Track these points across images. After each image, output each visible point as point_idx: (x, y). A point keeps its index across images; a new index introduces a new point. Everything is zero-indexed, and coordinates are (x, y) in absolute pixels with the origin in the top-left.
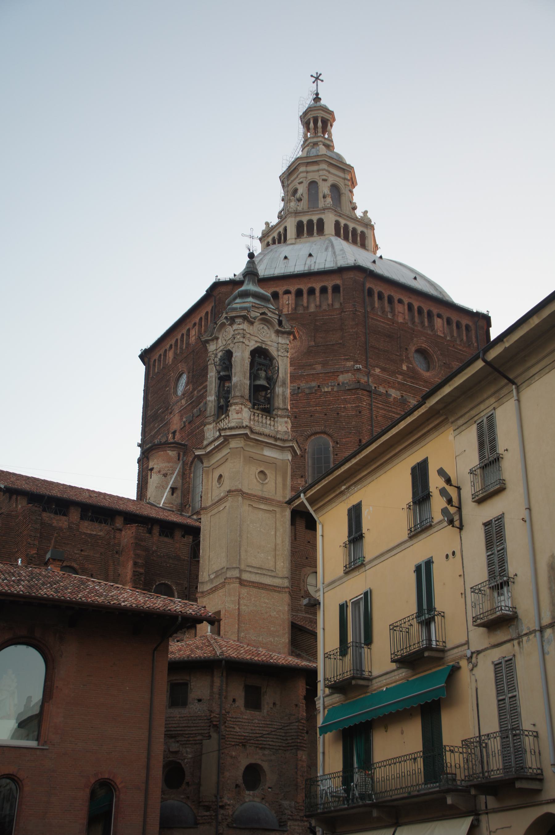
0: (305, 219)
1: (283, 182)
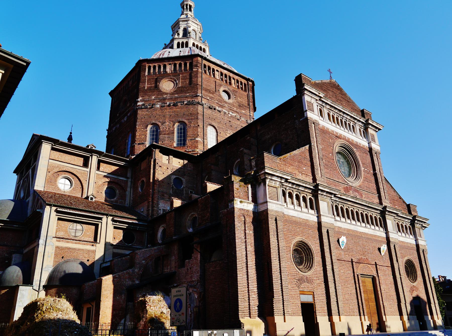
0: (181, 41)
1: (172, 29)
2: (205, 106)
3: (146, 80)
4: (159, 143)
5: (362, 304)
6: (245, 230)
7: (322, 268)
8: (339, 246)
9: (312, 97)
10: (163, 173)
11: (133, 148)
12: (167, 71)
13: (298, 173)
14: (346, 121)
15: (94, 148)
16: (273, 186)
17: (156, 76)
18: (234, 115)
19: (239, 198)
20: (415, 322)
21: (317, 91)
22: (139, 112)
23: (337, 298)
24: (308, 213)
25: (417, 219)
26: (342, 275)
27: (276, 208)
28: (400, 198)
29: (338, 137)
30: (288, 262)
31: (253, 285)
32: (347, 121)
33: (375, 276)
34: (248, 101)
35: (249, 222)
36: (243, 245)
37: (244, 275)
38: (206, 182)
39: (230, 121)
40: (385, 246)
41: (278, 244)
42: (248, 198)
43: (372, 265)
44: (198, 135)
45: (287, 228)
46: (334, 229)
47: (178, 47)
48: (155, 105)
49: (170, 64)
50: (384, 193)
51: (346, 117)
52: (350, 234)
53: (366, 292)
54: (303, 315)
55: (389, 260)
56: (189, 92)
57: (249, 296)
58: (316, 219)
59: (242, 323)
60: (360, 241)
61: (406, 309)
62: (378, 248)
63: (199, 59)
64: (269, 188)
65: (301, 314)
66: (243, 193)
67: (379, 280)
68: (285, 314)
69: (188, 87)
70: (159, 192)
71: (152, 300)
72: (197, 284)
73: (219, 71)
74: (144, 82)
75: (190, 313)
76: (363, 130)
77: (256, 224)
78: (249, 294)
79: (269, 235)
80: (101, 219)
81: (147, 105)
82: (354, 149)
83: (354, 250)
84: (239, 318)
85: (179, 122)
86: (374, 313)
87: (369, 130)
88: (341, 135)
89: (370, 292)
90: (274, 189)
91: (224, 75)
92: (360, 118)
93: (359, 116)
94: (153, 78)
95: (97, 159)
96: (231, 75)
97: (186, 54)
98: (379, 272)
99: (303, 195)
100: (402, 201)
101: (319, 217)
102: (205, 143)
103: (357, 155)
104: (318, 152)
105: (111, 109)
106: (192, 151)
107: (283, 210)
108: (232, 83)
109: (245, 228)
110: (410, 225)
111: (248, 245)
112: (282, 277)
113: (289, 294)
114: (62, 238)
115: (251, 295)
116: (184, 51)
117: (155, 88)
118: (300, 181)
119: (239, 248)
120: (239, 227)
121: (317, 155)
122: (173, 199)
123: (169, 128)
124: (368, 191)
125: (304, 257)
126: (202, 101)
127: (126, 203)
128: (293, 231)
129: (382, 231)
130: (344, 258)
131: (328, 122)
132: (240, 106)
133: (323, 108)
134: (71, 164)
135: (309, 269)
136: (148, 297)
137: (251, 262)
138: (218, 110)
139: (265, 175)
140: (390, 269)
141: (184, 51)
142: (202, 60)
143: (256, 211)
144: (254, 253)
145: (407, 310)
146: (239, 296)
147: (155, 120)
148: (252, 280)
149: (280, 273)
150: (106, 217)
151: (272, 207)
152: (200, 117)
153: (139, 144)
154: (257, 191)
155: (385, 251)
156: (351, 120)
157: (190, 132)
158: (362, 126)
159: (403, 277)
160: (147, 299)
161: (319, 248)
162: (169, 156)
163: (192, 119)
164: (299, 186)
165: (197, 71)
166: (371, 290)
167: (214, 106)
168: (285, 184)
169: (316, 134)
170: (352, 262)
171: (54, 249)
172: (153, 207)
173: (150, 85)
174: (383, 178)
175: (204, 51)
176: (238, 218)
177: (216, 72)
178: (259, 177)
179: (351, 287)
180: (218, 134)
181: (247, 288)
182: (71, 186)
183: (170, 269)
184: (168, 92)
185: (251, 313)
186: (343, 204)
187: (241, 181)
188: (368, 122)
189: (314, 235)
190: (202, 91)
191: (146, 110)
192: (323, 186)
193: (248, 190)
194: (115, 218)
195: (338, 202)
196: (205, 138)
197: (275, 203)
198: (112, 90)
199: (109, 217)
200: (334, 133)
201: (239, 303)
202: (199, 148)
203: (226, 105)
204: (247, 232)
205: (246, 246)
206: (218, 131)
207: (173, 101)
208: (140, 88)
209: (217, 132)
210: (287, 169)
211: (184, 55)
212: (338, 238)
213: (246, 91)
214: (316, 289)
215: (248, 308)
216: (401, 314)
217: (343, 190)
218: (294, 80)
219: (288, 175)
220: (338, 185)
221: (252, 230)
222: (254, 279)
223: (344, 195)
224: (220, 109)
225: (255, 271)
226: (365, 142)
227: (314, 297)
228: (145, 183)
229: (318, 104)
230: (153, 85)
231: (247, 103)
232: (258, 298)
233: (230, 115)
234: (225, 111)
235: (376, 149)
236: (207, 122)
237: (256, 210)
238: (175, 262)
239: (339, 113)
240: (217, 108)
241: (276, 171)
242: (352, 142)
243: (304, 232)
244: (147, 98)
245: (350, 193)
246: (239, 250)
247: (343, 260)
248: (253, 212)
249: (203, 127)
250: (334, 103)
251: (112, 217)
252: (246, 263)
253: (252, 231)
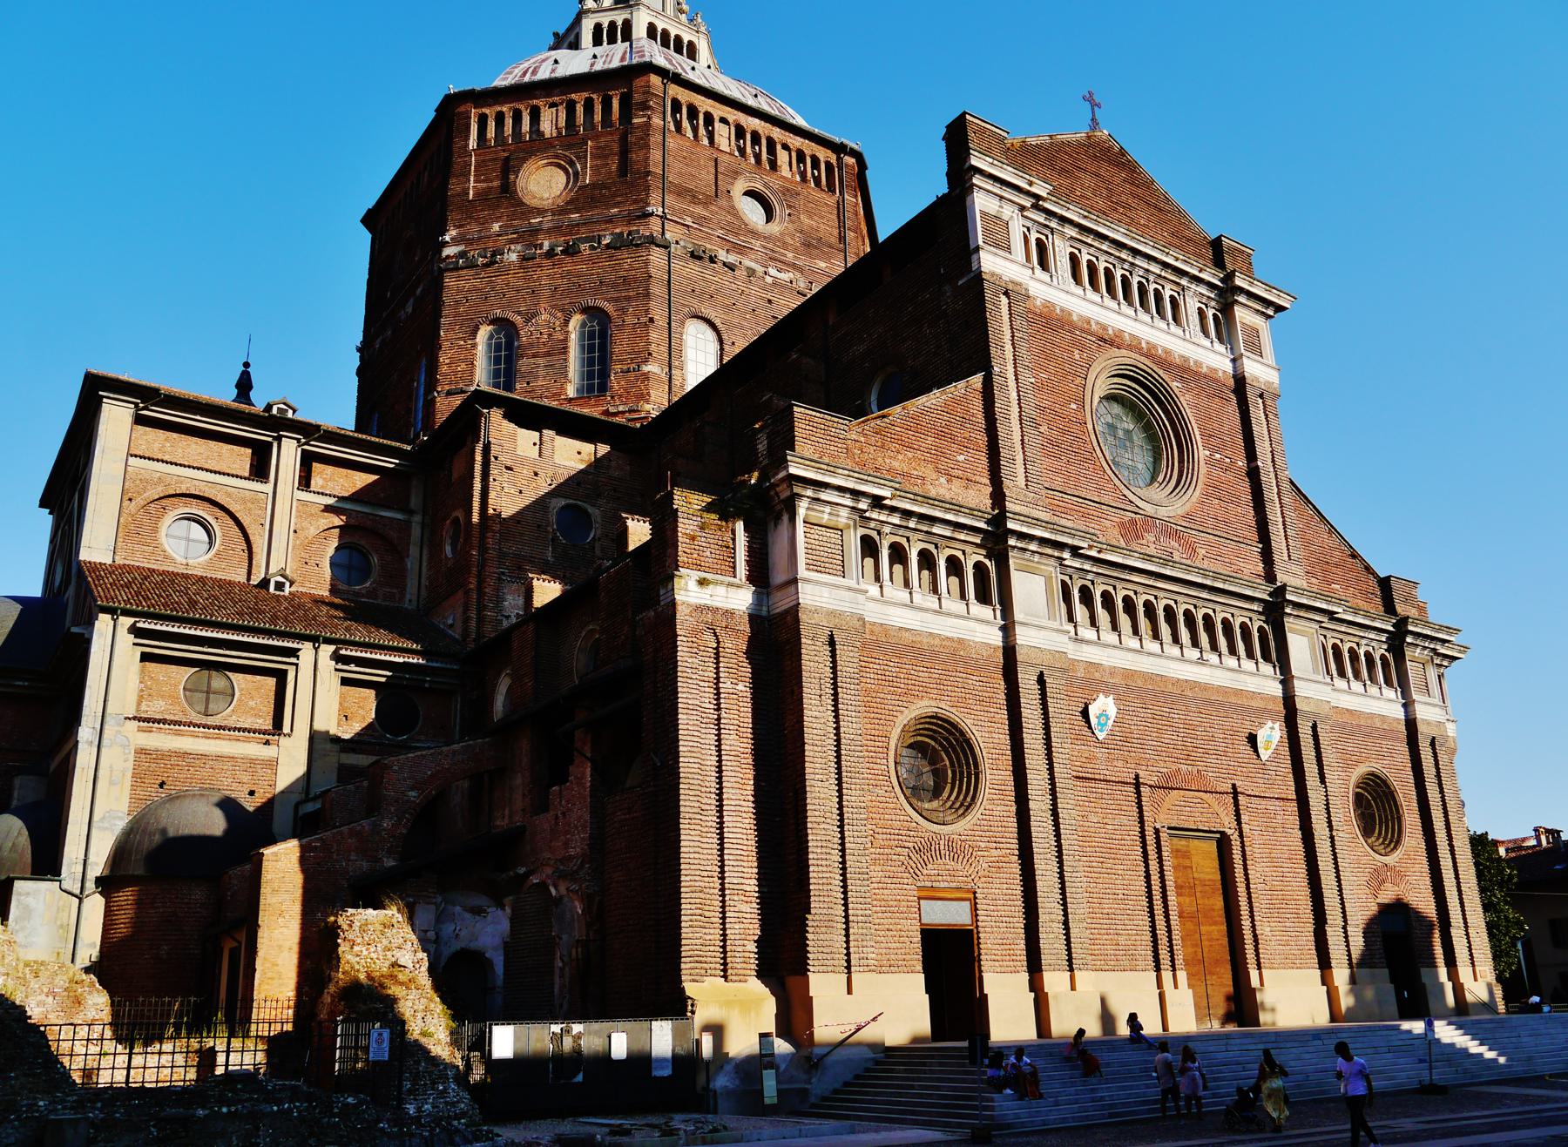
0: (605, 20)
2: (676, 249)
3: (473, 168)
4: (518, 386)
5: (1169, 931)
6: (718, 678)
7: (1014, 808)
8: (1086, 729)
9: (1002, 198)
10: (521, 492)
11: (430, 404)
12: (542, 129)
13: (934, 476)
14: (1144, 281)
15: (290, 412)
16: (824, 522)
17: (504, 151)
18: (785, 276)
19: (698, 567)
20: (1381, 987)
21: (1021, 174)
22: (450, 281)
23: (1065, 911)
24: (967, 616)
25: (1410, 628)
26: (1092, 830)
27: (831, 601)
28: (1354, 555)
29: (1109, 341)
30: (878, 790)
31: (741, 869)
32: (1148, 281)
33: (1229, 832)
34: (840, 227)
35: (734, 651)
36: (707, 731)
37: (709, 835)
38: (624, 515)
39: (770, 301)
41: (837, 728)
42: (734, 568)
43: (1220, 793)
44: (650, 354)
45: (879, 672)
46: (1064, 670)
47: (597, 41)
48: (503, 254)
49: (552, 105)
50: (1286, 539)
51: (1146, 266)
52: (1129, 688)
53: (1191, 887)
54: (926, 970)
55: (1291, 775)
56: (619, 203)
57: (723, 907)
58: (996, 638)
59: (689, 998)
60: (1176, 711)
61: (1348, 946)
62: (1250, 733)
63: (655, 80)
64: (809, 530)
65: (919, 967)
66: (713, 551)
67: (1243, 847)
68: (853, 969)
69: (614, 183)
70: (502, 555)
71: (358, 924)
72: (582, 866)
73: (731, 121)
74: (461, 175)
75: (560, 964)
76: (1214, 315)
77: (761, 658)
78: (723, 901)
79: (802, 698)
80: (294, 653)
81: (473, 256)
82: (1174, 385)
83: (1150, 743)
84: (681, 982)
85: (585, 310)
87: (1237, 313)
88: (1119, 333)
89: (1207, 888)
90: (828, 535)
91: (748, 137)
92: (1201, 270)
94: (495, 159)
95: (299, 449)
96: (777, 133)
97: (615, 63)
98: (1244, 818)
99: (948, 552)
100: (1360, 566)
101: (1008, 629)
102: (677, 383)
103: (1185, 406)
104: (1019, 396)
105: (369, 274)
106: (630, 411)
107: (861, 607)
108: (779, 163)
109: (717, 673)
110: (1386, 650)
111: (727, 732)
112: (847, 840)
113: (869, 900)
114: (164, 721)
115: (732, 903)
116: (607, 56)
117: (501, 193)
118: (931, 502)
119: (691, 744)
120: (694, 671)
121: (1015, 410)
122: (533, 579)
123: (550, 335)
124: (1219, 533)
125: (949, 772)
126: (663, 233)
127: (408, 596)
128: (902, 681)
129: (1267, 673)
130: (1104, 771)
131: (1066, 288)
132: (807, 245)
133: (1050, 236)
134: (207, 470)
135: (961, 812)
136: (349, 914)
137: (738, 791)
138: (724, 264)
139: (791, 486)
140: (1293, 807)
141: (607, 56)
142: (665, 84)
143: (764, 613)
144: (750, 761)
145: (1349, 951)
146: (683, 906)
147: (503, 308)
148: (739, 852)
149: (838, 827)
150: (314, 645)
151: (817, 598)
152: (657, 289)
153: (449, 393)
154: (770, 544)
155: (1274, 747)
156: (1165, 278)
157: (621, 346)
158: (1209, 297)
159: (1341, 834)
160: (340, 921)
161: (1005, 739)
162: (541, 432)
163: (628, 299)
164: (933, 520)
165: (647, 125)
166: (1209, 880)
167: (710, 250)
168: (874, 515)
169: (1013, 332)
170: (1137, 785)
171: (131, 757)
172: (481, 608)
173: (484, 185)
174: (1286, 486)
175: (692, 52)
176: (690, 639)
177: (717, 125)
178: (772, 493)
179: (1129, 873)
180: (726, 347)
181: (719, 878)
182: (211, 543)
183: (510, 817)
184: (547, 204)
185: (730, 965)
186: (1112, 581)
187: (709, 508)
188: (1233, 282)
189: (987, 695)
190: (663, 198)
191: (472, 272)
192: (1022, 518)
193: (734, 540)
194: (341, 649)
195: (1090, 577)
196: (677, 363)
197: (826, 584)
198: (369, 210)
199: (322, 645)
200: (1094, 326)
201: (683, 930)
202: (653, 398)
203: (757, 244)
204: (726, 686)
205: (719, 735)
206: (725, 336)
207: (565, 235)
208: (453, 196)
209: (721, 341)
210: (888, 461)
211: (606, 67)
212: (1086, 704)
213: (834, 192)
214: (983, 879)
215: (718, 948)
216: (1324, 963)
217: (1116, 532)
218: (943, 139)
219: (882, 482)
220: (1095, 513)
221: (748, 680)
222: (745, 848)
224: (732, 258)
225: (752, 821)
226: (1218, 357)
227: (975, 909)
228: (462, 527)
229: (1029, 224)
230: (496, 184)
231: (836, 232)
232: (759, 915)
233: (769, 280)
234: (753, 265)
236: (683, 305)
237: (765, 609)
238: (524, 795)
239: (1117, 254)
240: (722, 255)
241: (832, 469)
242: (1164, 356)
243: (945, 683)
244: (473, 229)
245: (1144, 542)
246: (689, 748)
247: (1100, 780)
248: (750, 615)
249: (669, 324)
250: (1095, 218)
251: (333, 648)
252: (717, 795)
253: (748, 684)
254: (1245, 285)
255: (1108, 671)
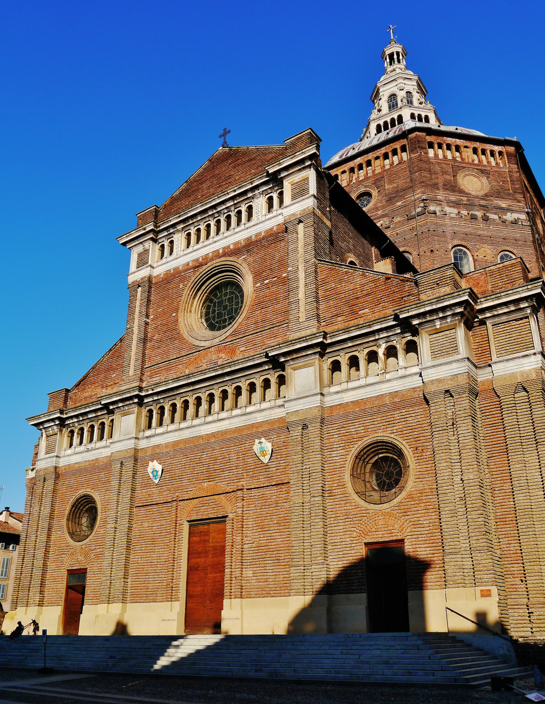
9: (141, 243)
21: (138, 229)
27: (45, 464)
40: (260, 443)
51: (224, 207)
86: (218, 594)
89: (217, 551)
93: (245, 184)
151: (41, 465)
158: (270, 188)
166: (220, 546)
192: (104, 397)
223: (156, 385)
235: (296, 213)
241: (39, 417)
250: (183, 213)
254: (277, 168)
255: (164, 446)
